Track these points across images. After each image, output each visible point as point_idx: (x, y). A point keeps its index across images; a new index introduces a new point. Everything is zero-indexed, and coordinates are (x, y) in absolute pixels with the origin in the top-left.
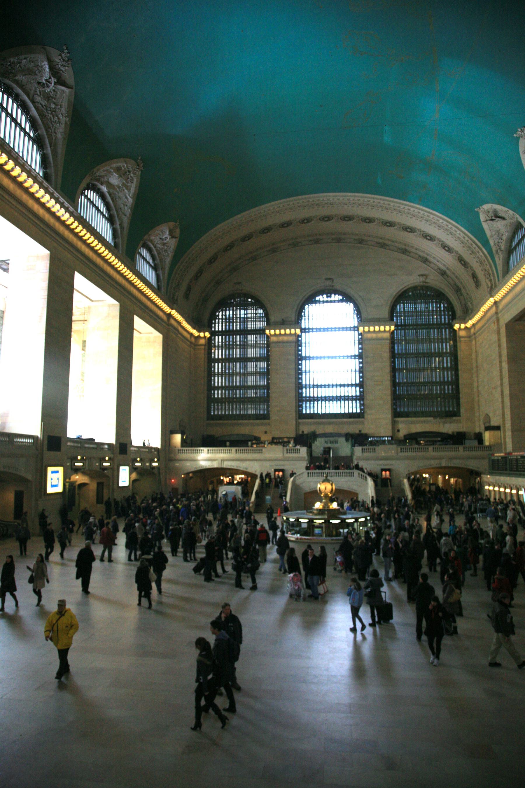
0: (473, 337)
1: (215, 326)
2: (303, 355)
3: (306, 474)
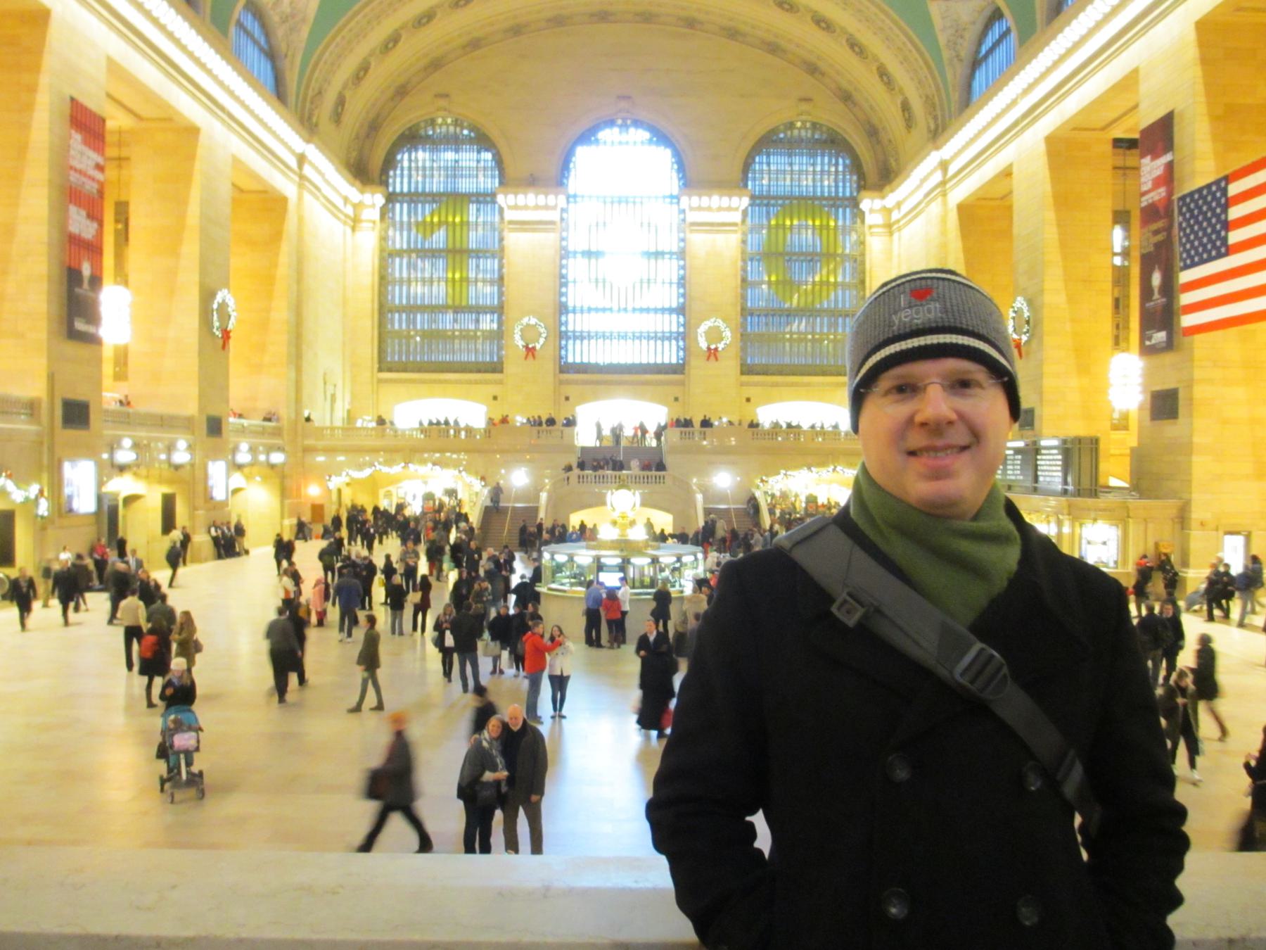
1: (394, 182)
2: (571, 249)
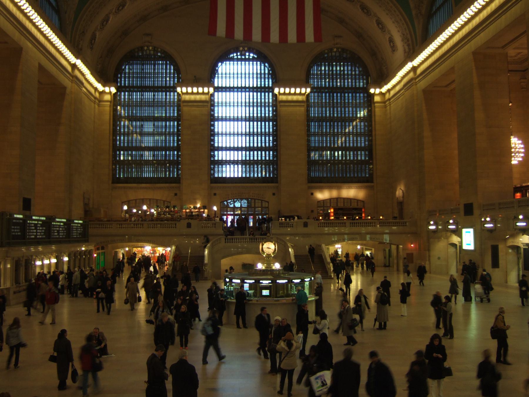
0: (387, 103)
1: (121, 81)
3: (223, 240)
